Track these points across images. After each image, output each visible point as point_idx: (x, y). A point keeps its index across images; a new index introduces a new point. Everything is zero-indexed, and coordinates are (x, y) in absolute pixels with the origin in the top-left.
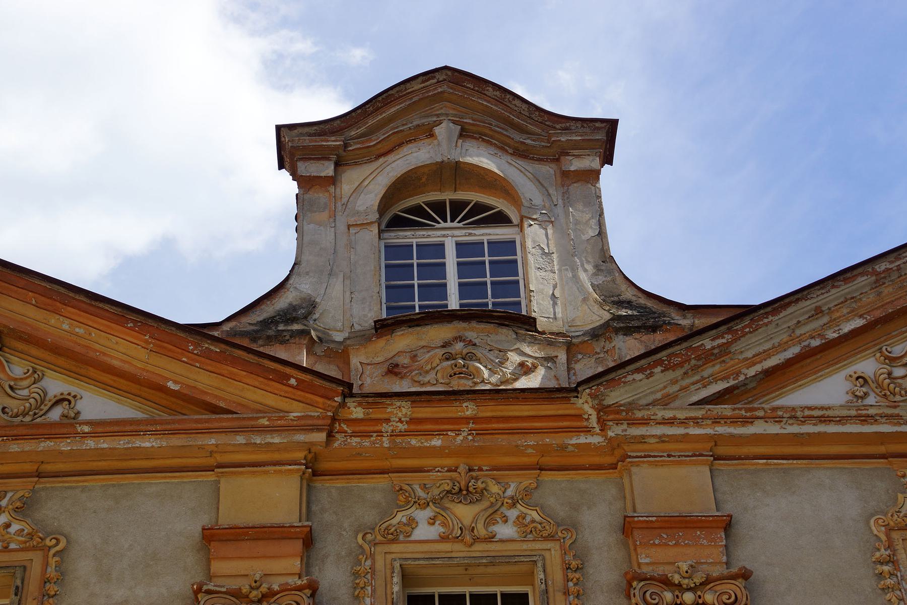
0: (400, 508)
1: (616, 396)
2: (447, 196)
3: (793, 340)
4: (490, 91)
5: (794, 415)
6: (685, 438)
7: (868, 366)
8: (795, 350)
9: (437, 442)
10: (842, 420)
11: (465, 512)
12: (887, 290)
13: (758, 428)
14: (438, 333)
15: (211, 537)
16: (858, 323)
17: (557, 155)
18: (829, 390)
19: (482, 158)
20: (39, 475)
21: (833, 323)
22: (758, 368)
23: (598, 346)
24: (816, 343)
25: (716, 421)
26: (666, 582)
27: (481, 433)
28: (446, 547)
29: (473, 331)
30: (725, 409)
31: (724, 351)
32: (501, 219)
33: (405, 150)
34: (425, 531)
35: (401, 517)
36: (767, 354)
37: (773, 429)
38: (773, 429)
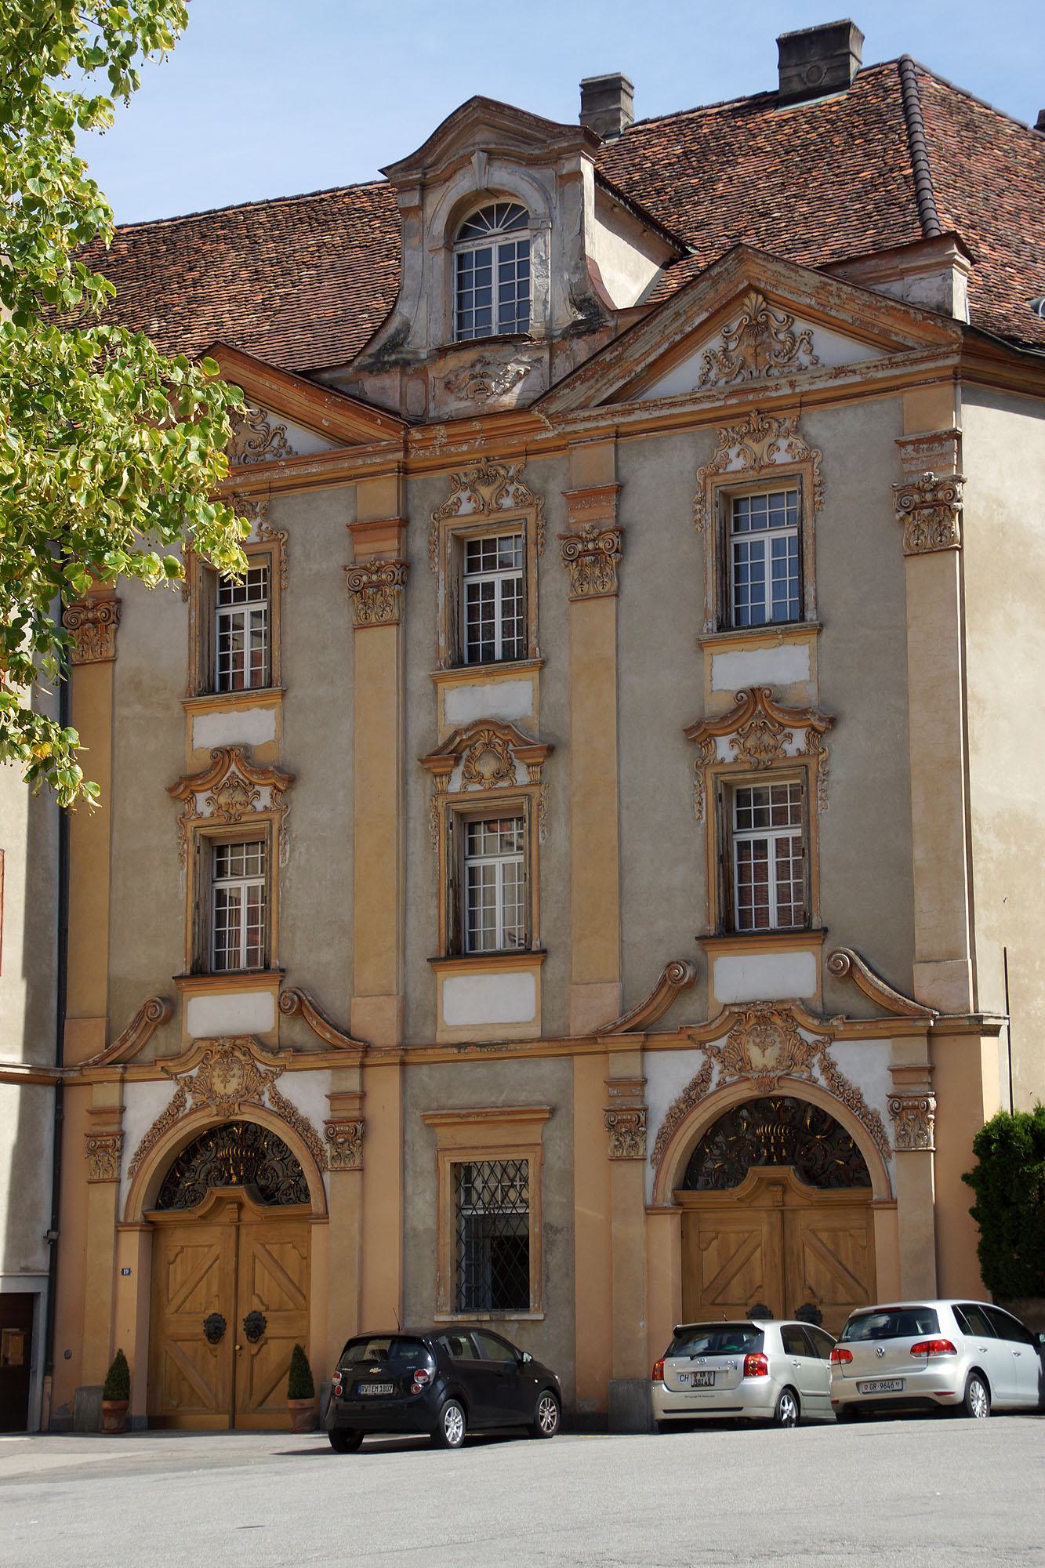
0: (453, 492)
1: (556, 407)
2: (494, 202)
3: (664, 339)
4: (507, 112)
6: (597, 428)
7: (715, 343)
8: (665, 346)
9: (465, 448)
10: (682, 403)
11: (486, 492)
12: (722, 286)
13: (638, 416)
14: (469, 356)
16: (705, 316)
17: (557, 158)
18: (685, 376)
19: (503, 176)
20: (270, 490)
22: (643, 365)
23: (567, 344)
24: (678, 338)
25: (614, 414)
27: (488, 438)
28: (475, 518)
29: (488, 353)
30: (617, 406)
31: (619, 359)
33: (458, 176)
34: (466, 508)
35: (453, 499)
36: (647, 353)
37: (645, 415)
38: (645, 415)
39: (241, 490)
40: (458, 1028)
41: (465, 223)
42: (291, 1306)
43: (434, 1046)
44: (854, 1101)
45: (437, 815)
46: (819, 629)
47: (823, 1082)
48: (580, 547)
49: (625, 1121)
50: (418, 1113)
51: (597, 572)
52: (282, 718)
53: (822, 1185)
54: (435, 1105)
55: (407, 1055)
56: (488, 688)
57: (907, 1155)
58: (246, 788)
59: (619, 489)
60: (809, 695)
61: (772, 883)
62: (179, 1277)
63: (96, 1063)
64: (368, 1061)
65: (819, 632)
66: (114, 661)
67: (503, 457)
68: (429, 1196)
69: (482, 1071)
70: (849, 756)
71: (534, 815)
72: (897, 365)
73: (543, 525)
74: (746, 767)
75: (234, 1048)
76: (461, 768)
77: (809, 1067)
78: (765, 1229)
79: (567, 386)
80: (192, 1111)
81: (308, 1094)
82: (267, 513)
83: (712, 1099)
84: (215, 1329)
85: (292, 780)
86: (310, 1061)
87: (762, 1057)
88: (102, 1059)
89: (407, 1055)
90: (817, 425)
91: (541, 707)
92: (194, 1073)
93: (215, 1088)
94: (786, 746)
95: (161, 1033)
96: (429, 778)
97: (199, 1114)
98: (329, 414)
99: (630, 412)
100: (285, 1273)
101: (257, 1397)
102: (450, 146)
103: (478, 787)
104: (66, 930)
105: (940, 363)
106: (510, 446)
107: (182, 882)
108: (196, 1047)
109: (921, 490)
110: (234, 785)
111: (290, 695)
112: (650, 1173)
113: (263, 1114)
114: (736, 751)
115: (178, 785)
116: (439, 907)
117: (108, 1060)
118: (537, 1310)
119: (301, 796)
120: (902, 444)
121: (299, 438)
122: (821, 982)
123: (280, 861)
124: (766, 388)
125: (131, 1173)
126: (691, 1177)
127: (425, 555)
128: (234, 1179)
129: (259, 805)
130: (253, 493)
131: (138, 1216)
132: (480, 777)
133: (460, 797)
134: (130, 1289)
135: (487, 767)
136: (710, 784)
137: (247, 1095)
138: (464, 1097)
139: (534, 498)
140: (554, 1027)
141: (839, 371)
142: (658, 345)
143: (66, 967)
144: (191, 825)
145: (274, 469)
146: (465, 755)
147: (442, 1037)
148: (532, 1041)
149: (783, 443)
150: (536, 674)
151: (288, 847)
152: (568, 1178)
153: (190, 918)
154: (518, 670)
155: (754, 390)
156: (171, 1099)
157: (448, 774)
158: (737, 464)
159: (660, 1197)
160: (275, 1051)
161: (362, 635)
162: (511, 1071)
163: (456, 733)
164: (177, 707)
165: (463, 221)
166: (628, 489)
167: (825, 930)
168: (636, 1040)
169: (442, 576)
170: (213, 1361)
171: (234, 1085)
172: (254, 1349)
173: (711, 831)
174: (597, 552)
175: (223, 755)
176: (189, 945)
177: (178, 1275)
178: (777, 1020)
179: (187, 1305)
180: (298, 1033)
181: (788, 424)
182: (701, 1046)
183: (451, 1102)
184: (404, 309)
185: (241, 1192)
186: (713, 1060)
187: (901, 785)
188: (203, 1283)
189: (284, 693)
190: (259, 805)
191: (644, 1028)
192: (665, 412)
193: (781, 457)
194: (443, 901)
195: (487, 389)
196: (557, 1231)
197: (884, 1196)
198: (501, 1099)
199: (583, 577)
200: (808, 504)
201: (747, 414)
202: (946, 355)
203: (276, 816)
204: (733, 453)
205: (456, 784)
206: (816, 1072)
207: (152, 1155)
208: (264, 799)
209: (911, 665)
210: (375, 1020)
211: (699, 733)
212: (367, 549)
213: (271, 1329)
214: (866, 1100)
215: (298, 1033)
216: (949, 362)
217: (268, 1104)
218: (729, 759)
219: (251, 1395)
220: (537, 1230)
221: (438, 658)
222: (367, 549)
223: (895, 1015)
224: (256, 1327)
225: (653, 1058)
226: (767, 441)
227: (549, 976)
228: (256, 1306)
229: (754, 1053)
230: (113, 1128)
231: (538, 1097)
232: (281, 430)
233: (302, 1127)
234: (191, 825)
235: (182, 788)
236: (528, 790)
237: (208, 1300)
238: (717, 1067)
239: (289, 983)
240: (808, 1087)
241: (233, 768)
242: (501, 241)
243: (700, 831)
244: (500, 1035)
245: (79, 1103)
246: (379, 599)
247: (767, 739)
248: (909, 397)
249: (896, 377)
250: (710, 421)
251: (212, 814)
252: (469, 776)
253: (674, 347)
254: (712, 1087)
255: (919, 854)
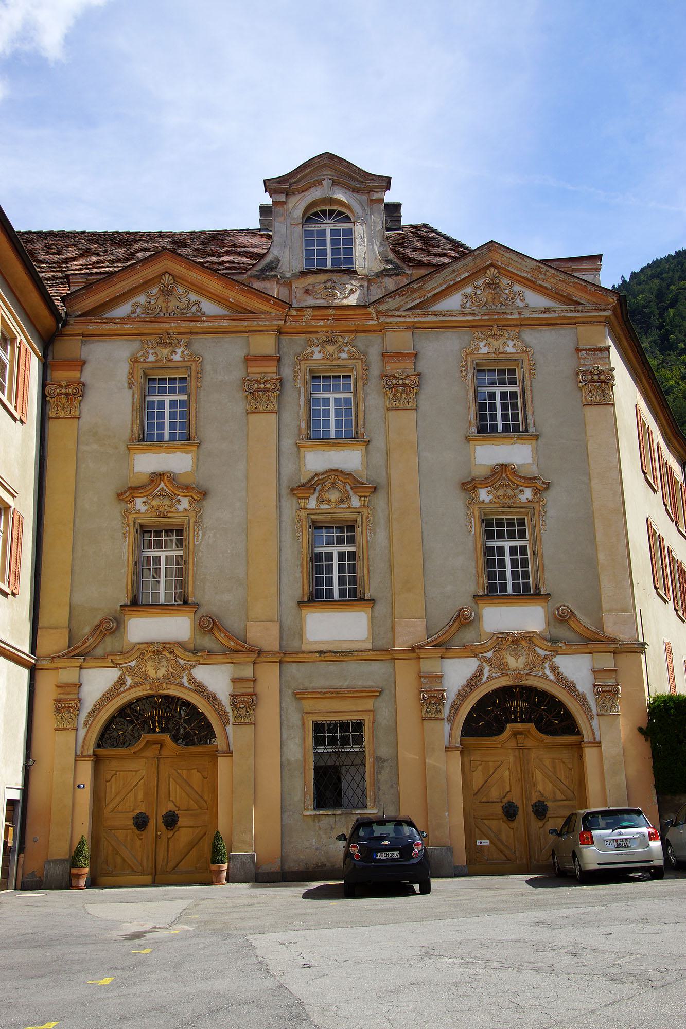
0: (309, 347)
1: (382, 307)
2: (328, 208)
3: (445, 282)
4: (344, 163)
5: (441, 313)
6: (405, 322)
7: (469, 290)
8: (445, 286)
9: (321, 323)
10: (456, 315)
11: (330, 349)
12: (478, 261)
13: (429, 318)
14: (322, 277)
15: (249, 359)
16: (467, 274)
17: (369, 191)
18: (453, 302)
19: (341, 196)
20: (191, 333)
21: (459, 275)
22: (432, 293)
23: (379, 280)
24: (452, 283)
25: (416, 316)
26: (394, 377)
27: (336, 320)
28: (324, 362)
29: (335, 277)
30: (419, 312)
31: (420, 288)
32: (347, 219)
33: (312, 190)
34: (317, 356)
35: (309, 350)
36: (435, 288)
37: (434, 319)
38: (434, 319)
39: (171, 331)
40: (317, 642)
41: (311, 216)
42: (196, 807)
43: (304, 653)
44: (570, 688)
45: (301, 520)
46: (537, 437)
47: (551, 677)
48: (394, 382)
49: (431, 700)
50: (290, 692)
51: (404, 396)
52: (197, 459)
53: (553, 734)
54: (301, 687)
55: (284, 657)
56: (332, 453)
57: (605, 717)
58: (172, 497)
59: (416, 355)
60: (533, 471)
61: (508, 569)
62: (113, 790)
63: (63, 656)
64: (259, 660)
65: (537, 440)
66: (79, 418)
67: (341, 332)
68: (298, 741)
69: (333, 668)
70: (556, 504)
71: (364, 524)
72: (578, 311)
73: (366, 369)
74: (498, 505)
75: (161, 650)
76: (316, 495)
77: (544, 668)
78: (512, 759)
79: (391, 297)
80: (131, 687)
81: (217, 679)
82: (188, 346)
83: (485, 686)
84: (141, 822)
85: (204, 494)
86: (220, 658)
87: (515, 662)
88: (68, 653)
89: (284, 657)
90: (530, 336)
91: (367, 466)
92: (133, 664)
93: (148, 673)
94: (520, 496)
95: (108, 640)
96: (295, 500)
97: (136, 689)
98: (234, 296)
99: (426, 316)
100: (192, 787)
101: (172, 864)
102: (306, 175)
103: (327, 507)
104: (40, 574)
105: (601, 314)
106: (349, 326)
107: (125, 549)
108: (136, 648)
109: (592, 373)
110: (165, 495)
111: (203, 446)
112: (447, 727)
113: (183, 690)
114: (491, 497)
115: (125, 492)
116: (302, 572)
117: (72, 654)
118: (373, 807)
119: (209, 505)
120: (578, 350)
121: (209, 307)
122: (548, 623)
123: (195, 539)
124: (505, 314)
125: (85, 725)
126: (107, 737)
127: (291, 378)
128: (158, 729)
129: (181, 508)
130: (179, 334)
131: (91, 752)
132: (328, 501)
133: (316, 511)
134: (85, 797)
135: (334, 496)
136: (476, 513)
137: (169, 679)
138: (320, 683)
139: (362, 355)
140: (380, 643)
141: (546, 310)
142: (441, 285)
143: (39, 597)
144: (132, 517)
145: (198, 321)
146: (318, 488)
147: (305, 647)
148: (369, 651)
149: (511, 343)
150: (364, 448)
151: (200, 533)
152: (394, 730)
153: (130, 571)
154: (353, 445)
155: (498, 314)
156: (116, 679)
157: (308, 498)
158: (484, 350)
159: (454, 741)
160: (194, 652)
161: (252, 417)
162: (352, 668)
163: (316, 475)
164: (123, 448)
165: (308, 214)
166: (420, 356)
167: (549, 595)
168: (438, 652)
169: (303, 390)
170: (139, 843)
171: (162, 672)
172: (170, 834)
173: (478, 539)
174: (405, 385)
175: (157, 477)
176: (129, 587)
177: (112, 788)
178: (524, 643)
179: (120, 807)
180: (207, 642)
181: (513, 333)
182: (476, 655)
183: (311, 685)
184: (275, 252)
185: (167, 738)
186: (484, 664)
187: (589, 521)
188: (132, 793)
189: (199, 445)
190: (181, 508)
191: (443, 646)
192: (445, 318)
193: (510, 349)
194: (305, 569)
195: (334, 295)
196: (385, 761)
197: (591, 740)
198: (346, 684)
199: (395, 398)
200: (527, 374)
201: (492, 326)
202: (605, 310)
203: (193, 515)
204: (482, 344)
205: (312, 503)
206: (547, 671)
207: (102, 713)
208: (185, 504)
209: (591, 462)
210: (264, 635)
211: (469, 486)
212: (256, 371)
213: (182, 822)
214: (578, 687)
215: (207, 642)
216: (605, 314)
217: (186, 684)
218: (487, 501)
219: (167, 863)
220: (371, 760)
221: (300, 434)
222: (256, 371)
223: (592, 641)
224: (171, 821)
225: (448, 662)
226: (502, 341)
227: (376, 614)
228: (171, 807)
229: (512, 662)
230: (74, 696)
231: (370, 683)
232: (197, 303)
233: (212, 699)
234: (132, 517)
235: (128, 494)
236: (360, 510)
237: (135, 803)
238: (487, 668)
239: (202, 612)
240: (542, 680)
241: (162, 485)
242: (333, 227)
243: (471, 538)
244: (345, 647)
245: (47, 682)
246: (265, 398)
247: (509, 491)
248: (581, 329)
249: (576, 317)
250: (469, 327)
251: (147, 511)
252: (321, 500)
253: (449, 287)
254: (484, 679)
255: (601, 557)
